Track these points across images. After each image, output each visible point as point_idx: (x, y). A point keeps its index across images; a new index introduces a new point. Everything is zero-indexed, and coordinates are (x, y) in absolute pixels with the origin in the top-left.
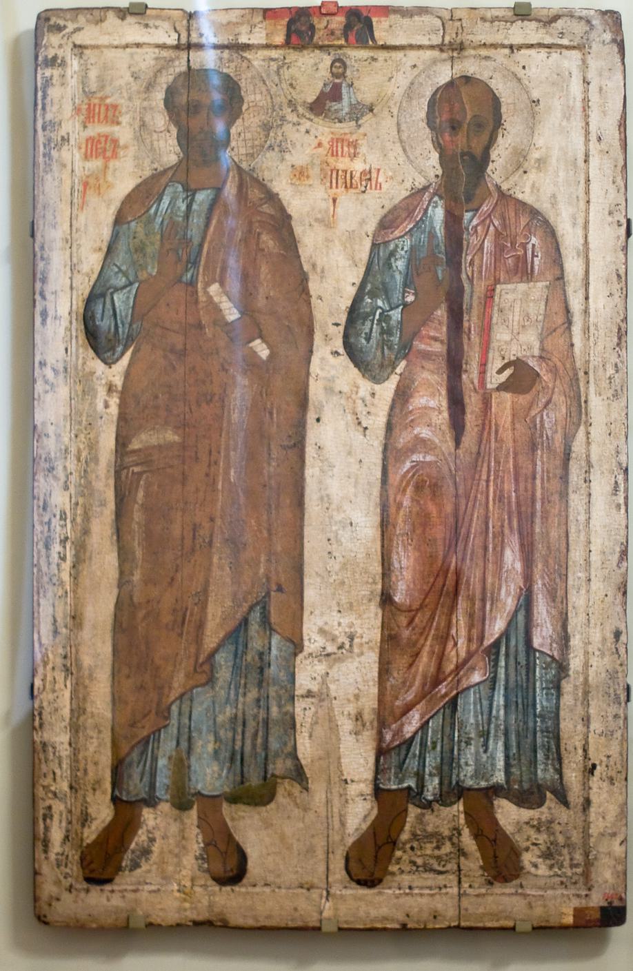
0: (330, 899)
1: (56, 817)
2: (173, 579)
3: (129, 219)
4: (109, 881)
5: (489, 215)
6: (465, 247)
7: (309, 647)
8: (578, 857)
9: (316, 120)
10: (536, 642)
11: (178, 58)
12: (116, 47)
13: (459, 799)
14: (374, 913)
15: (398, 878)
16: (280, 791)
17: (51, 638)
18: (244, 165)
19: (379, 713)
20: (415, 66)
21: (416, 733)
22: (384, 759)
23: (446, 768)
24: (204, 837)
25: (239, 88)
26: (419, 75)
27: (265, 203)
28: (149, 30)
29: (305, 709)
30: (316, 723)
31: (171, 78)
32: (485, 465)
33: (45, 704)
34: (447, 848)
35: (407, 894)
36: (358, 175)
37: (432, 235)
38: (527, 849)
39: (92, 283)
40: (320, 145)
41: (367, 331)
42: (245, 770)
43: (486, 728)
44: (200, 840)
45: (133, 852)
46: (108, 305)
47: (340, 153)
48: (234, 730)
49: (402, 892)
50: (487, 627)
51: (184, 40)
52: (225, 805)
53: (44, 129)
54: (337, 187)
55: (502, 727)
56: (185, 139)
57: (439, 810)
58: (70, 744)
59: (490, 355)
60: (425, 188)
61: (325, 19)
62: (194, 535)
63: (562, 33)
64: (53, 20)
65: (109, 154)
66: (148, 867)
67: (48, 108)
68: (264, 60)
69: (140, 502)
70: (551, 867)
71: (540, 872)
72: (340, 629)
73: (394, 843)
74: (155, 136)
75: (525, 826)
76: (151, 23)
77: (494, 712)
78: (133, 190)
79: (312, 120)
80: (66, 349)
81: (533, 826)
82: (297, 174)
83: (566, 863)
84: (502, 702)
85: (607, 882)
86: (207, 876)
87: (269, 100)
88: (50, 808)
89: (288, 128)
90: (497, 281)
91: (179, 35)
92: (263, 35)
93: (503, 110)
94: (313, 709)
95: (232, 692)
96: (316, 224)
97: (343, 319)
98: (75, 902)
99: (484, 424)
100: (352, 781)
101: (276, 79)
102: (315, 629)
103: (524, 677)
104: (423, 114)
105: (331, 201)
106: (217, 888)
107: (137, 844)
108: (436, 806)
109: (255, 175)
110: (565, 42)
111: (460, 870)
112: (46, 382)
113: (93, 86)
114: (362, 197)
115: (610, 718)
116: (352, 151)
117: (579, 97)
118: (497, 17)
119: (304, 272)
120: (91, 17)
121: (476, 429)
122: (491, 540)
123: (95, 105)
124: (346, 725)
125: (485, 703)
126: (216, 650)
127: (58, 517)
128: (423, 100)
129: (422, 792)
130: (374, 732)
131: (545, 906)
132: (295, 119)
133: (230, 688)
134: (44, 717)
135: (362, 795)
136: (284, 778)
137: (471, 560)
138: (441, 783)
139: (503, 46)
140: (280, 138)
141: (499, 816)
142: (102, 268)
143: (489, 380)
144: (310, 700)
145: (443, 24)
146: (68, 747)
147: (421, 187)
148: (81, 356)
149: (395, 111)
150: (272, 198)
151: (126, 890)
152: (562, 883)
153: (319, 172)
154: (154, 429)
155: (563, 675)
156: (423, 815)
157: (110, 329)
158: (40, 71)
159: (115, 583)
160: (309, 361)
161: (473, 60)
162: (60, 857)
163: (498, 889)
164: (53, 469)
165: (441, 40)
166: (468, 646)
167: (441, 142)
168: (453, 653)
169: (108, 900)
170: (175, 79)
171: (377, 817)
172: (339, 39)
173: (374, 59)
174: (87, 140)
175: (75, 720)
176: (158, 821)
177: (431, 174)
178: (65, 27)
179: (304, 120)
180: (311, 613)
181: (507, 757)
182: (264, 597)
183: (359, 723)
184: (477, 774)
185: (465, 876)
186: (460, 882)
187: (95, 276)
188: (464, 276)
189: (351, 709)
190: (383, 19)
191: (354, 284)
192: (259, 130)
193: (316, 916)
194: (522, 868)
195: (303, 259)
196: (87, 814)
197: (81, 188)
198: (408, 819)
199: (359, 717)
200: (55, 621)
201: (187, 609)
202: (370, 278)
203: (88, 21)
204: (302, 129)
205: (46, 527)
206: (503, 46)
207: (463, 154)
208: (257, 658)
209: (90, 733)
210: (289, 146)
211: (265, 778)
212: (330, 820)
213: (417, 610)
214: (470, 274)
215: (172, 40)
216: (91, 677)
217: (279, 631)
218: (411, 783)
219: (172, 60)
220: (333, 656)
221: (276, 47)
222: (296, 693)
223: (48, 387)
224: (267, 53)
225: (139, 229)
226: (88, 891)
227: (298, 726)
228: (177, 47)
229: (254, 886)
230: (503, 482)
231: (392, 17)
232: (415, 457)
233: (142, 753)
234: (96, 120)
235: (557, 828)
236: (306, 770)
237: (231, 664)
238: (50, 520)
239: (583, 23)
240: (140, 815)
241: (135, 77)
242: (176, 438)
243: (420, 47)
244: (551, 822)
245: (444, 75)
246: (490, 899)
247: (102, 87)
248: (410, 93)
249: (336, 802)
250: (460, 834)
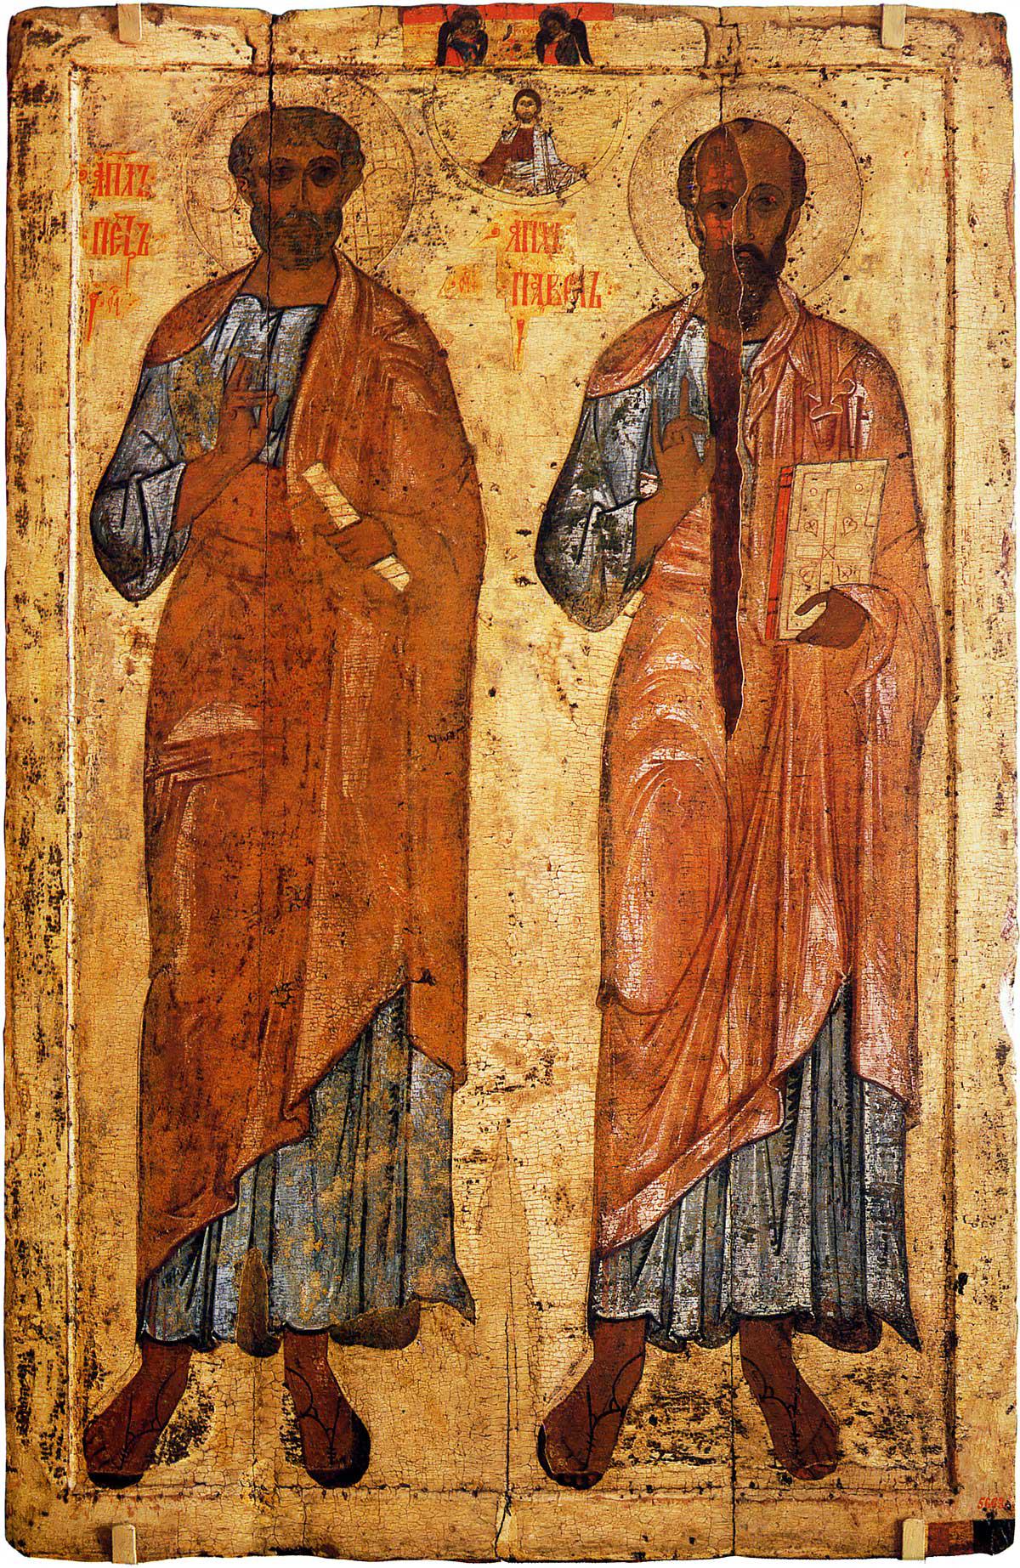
1: (42, 1371)
2: (243, 962)
3: (170, 356)
4: (134, 1480)
5: (785, 350)
6: (742, 404)
7: (477, 1076)
8: (937, 1434)
9: (489, 191)
10: (865, 1066)
13: (733, 1334)
15: (627, 1472)
16: (427, 1321)
18: (366, 267)
19: (596, 1186)
20: (658, 102)
21: (659, 1221)
22: (606, 1267)
23: (710, 1281)
25: (358, 139)
27: (402, 330)
28: (202, 40)
29: (470, 1182)
31: (241, 122)
32: (777, 766)
34: (713, 1418)
35: (645, 1500)
37: (687, 383)
38: (849, 1422)
39: (104, 464)
40: (495, 232)
41: (577, 543)
42: (367, 1286)
43: (778, 1213)
44: (289, 1408)
45: (174, 1429)
46: (133, 501)
47: (530, 246)
48: (350, 1221)
49: (635, 1496)
50: (780, 1039)
51: (262, 58)
52: (332, 1347)
55: (806, 1211)
56: (265, 223)
59: (786, 583)
60: (675, 306)
62: (280, 886)
64: (39, 23)
65: (133, 248)
66: (199, 1455)
70: (890, 1452)
72: (530, 1045)
73: (623, 1411)
74: (213, 217)
75: (846, 1382)
77: (793, 1185)
78: (176, 308)
80: (61, 575)
81: (861, 1382)
82: (457, 281)
83: (916, 1445)
84: (806, 1169)
88: (31, 1354)
90: (798, 460)
91: (254, 51)
93: (810, 173)
95: (345, 1153)
97: (535, 523)
99: (774, 699)
100: (551, 1306)
103: (844, 1126)
104: (672, 181)
105: (515, 325)
108: (694, 1347)
114: (567, 318)
115: (990, 1195)
119: (469, 445)
121: (761, 707)
122: (787, 893)
124: (542, 1209)
125: (777, 1170)
126: (317, 1083)
127: (46, 858)
129: (671, 1322)
130: (588, 1220)
132: (454, 190)
134: (21, 1200)
136: (432, 1301)
137: (753, 926)
138: (702, 1307)
139: (810, 68)
141: (800, 1365)
143: (783, 624)
144: (477, 1166)
145: (706, 33)
147: (667, 303)
148: (87, 586)
149: (624, 176)
150: (413, 320)
155: (910, 1121)
156: (672, 1361)
157: (135, 541)
158: (14, 109)
163: (799, 1488)
164: (38, 776)
166: (748, 1074)
168: (723, 1084)
172: (527, 57)
173: (588, 90)
177: (686, 281)
178: (58, 36)
180: (481, 1017)
181: (815, 1262)
182: (400, 991)
184: (762, 1293)
187: (110, 452)
188: (739, 450)
189: (548, 1180)
190: (604, 23)
191: (554, 464)
194: (841, 1454)
196: (95, 1366)
197: (87, 305)
200: (41, 1034)
201: (267, 1014)
202: (581, 455)
204: (466, 206)
205: (26, 878)
206: (810, 68)
207: (740, 249)
208: (387, 1093)
211: (401, 1301)
213: (661, 1012)
214: (752, 449)
215: (242, 60)
218: (652, 1307)
220: (517, 1091)
221: (420, 70)
222: (454, 1155)
223: (29, 639)
225: (186, 374)
228: (249, 71)
229: (382, 1487)
230: (807, 796)
232: (657, 754)
233: (190, 1258)
234: (112, 191)
235: (902, 1385)
238: (33, 862)
240: (186, 1366)
244: (890, 1374)
245: (707, 117)
246: (787, 1508)
249: (523, 1345)
250: (734, 1395)
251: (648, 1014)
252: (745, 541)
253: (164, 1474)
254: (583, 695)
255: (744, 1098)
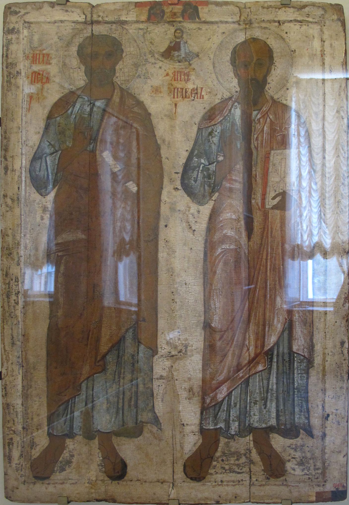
0: (174, 488)
1: (15, 445)
2: (81, 315)
3: (56, 116)
4: (48, 478)
5: (267, 113)
6: (253, 130)
7: (161, 352)
8: (319, 464)
9: (165, 61)
10: (295, 348)
11: (85, 29)
12: (49, 23)
13: (250, 434)
14: (200, 496)
15: (215, 476)
16: (145, 430)
17: (10, 347)
18: (124, 87)
19: (203, 387)
20: (224, 33)
21: (224, 398)
22: (206, 413)
23: (242, 417)
24: (102, 454)
25: (121, 45)
26: (226, 37)
27: (136, 106)
28: (68, 13)
29: (159, 386)
30: (166, 393)
31: (81, 40)
32: (265, 250)
33: (8, 383)
34: (243, 460)
35: (220, 485)
36: (190, 91)
37: (233, 124)
38: (289, 461)
39: (34, 151)
40: (167, 75)
41: (195, 176)
42: (125, 418)
43: (265, 395)
44: (100, 456)
45: (61, 462)
46: (44, 164)
47: (179, 79)
48: (118, 397)
49: (216, 484)
50: (266, 340)
51: (89, 19)
52: (114, 438)
53: (7, 68)
54: (177, 98)
55: (275, 395)
56: (89, 73)
57: (238, 440)
58: (22, 405)
59: (268, 190)
60: (230, 98)
61: (171, 7)
62: (94, 290)
63: (308, 14)
64: (13, 9)
65: (44, 80)
66: (70, 470)
67: (9, 56)
68: (135, 29)
69: (62, 272)
70: (303, 470)
71: (296, 473)
72: (179, 342)
73: (212, 458)
74: (71, 71)
75: (288, 448)
76: (69, 9)
77: (270, 387)
78: (58, 100)
79: (162, 61)
80: (19, 188)
81: (293, 448)
82: (154, 91)
83: (312, 468)
84: (275, 381)
85: (335, 477)
86: (105, 475)
87: (138, 51)
88: (11, 439)
89: (148, 66)
90: (272, 149)
91: (86, 16)
92: (135, 15)
93: (275, 55)
94: (163, 386)
95: (117, 377)
96: (165, 118)
97: (180, 170)
98: (28, 489)
99: (264, 228)
100: (187, 425)
101: (142, 40)
102: (164, 342)
103: (288, 367)
104: (228, 58)
105: (174, 105)
106: (110, 481)
107: (63, 458)
108: (236, 438)
109: (130, 92)
110: (310, 19)
111: (250, 472)
112: (7, 206)
113: (36, 44)
114: (192, 103)
115: (338, 389)
116: (186, 78)
117: (319, 49)
118: (270, 6)
119: (158, 144)
120: (34, 7)
121: (260, 231)
122: (268, 292)
123: (36, 54)
124: (183, 394)
125: (265, 382)
126: (107, 354)
127: (14, 280)
128: (228, 50)
129: (229, 430)
130: (200, 398)
131: (299, 492)
132: (153, 61)
133: (115, 375)
134: (7, 390)
135: (193, 432)
136: (147, 423)
137: (257, 303)
138: (239, 425)
139: (275, 21)
140: (145, 71)
141: (273, 443)
142: (40, 143)
143: (267, 203)
144: (162, 381)
145: (240, 11)
146: (21, 407)
147: (227, 97)
148: (28, 192)
149: (212, 56)
150: (140, 104)
151: (57, 483)
152: (309, 478)
153: (167, 89)
154: (70, 231)
155: (310, 366)
156: (229, 442)
157: (44, 176)
158: (5, 36)
159: (48, 316)
160: (160, 194)
161: (257, 29)
162: (18, 466)
163: (272, 481)
164: (11, 254)
165: (238, 19)
166: (255, 350)
167: (239, 73)
168: (247, 354)
169: (46, 489)
170: (84, 40)
171: (202, 445)
172: (178, 17)
173: (200, 29)
174: (32, 73)
175: (25, 391)
176: (76, 445)
177: (234, 90)
178: (20, 12)
179: (158, 61)
180: (162, 333)
181: (277, 411)
182: (134, 324)
183: (191, 393)
184: (260, 421)
185: (254, 475)
186: (250, 478)
187: (36, 148)
188: (253, 146)
189: (186, 385)
190: (205, 7)
191: (187, 150)
192: (132, 67)
193: (166, 497)
194: (286, 471)
195: (157, 138)
196: (33, 442)
197: (29, 100)
198: (220, 445)
199: (191, 390)
200: (13, 338)
201: (90, 331)
202: (197, 147)
203: (32, 8)
204: (157, 66)
205: (7, 286)
206: (275, 21)
207: (252, 79)
208: (130, 358)
209: (35, 399)
210: (150, 75)
211: (136, 423)
212: (174, 445)
213: (225, 331)
215: (81, 19)
216: (34, 368)
217: (143, 343)
218: (222, 425)
219: (82, 30)
220: (175, 357)
221: (142, 22)
222: (154, 377)
223: (8, 209)
224: (137, 25)
225: (62, 121)
226: (34, 483)
227: (155, 395)
228: (85, 23)
229: (131, 481)
230: (275, 260)
231: (210, 6)
232: (224, 247)
233: (65, 410)
234: (37, 62)
235: (307, 449)
236: (160, 418)
237: (115, 361)
238: (9, 282)
239: (321, 9)
240: (64, 443)
241: (60, 38)
242: (84, 237)
243: (227, 22)
244: (303, 446)
245: (241, 38)
246: (267, 488)
247: (41, 44)
248: (221, 46)
249: (178, 437)
250: (250, 452)
251: (221, 332)
252: (254, 176)
253: (58, 476)
254: (197, 227)
255: (254, 359)
